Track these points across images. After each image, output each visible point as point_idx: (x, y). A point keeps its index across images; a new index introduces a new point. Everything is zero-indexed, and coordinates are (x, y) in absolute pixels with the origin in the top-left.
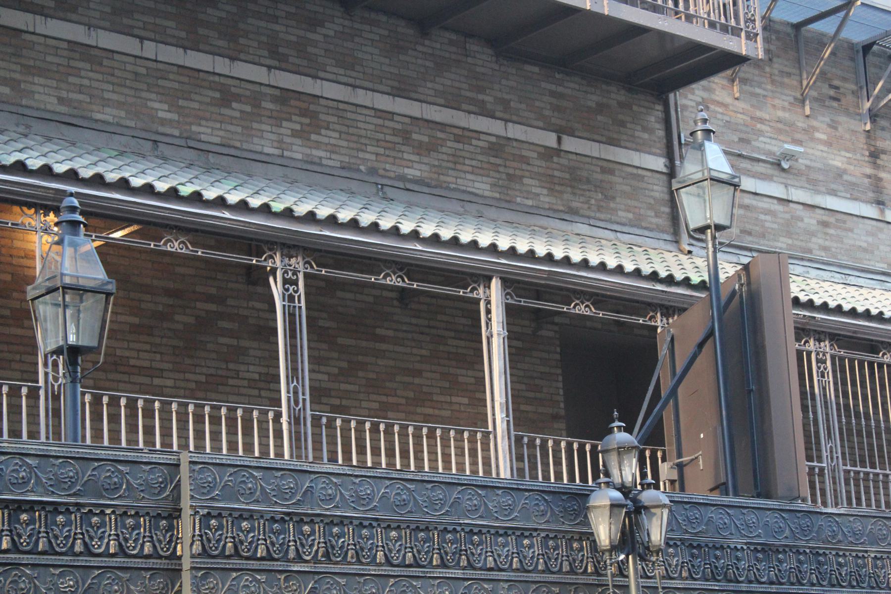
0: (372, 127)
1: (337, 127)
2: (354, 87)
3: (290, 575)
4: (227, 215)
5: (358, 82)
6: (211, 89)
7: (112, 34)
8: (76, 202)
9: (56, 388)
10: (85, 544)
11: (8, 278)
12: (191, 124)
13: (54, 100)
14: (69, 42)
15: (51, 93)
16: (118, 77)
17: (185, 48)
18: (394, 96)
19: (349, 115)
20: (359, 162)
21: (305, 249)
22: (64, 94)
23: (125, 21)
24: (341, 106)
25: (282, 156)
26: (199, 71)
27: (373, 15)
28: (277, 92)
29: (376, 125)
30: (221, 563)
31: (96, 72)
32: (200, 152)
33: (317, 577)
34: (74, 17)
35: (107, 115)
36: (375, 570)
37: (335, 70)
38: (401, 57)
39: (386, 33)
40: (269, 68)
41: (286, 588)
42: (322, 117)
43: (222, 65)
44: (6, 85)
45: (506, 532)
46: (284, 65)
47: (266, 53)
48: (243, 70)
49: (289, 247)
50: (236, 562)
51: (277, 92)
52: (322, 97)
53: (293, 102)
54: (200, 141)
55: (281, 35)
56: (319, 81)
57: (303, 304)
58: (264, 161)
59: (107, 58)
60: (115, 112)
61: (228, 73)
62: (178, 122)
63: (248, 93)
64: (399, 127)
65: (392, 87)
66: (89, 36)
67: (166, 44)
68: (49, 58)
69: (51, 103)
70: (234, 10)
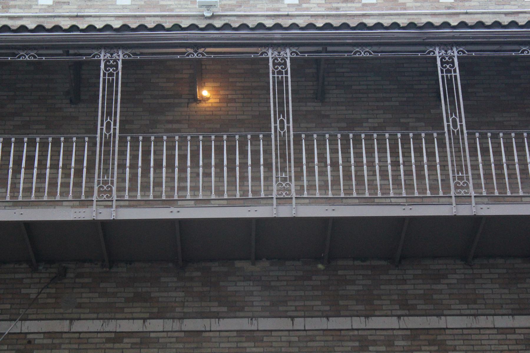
0: (496, 342)
1: (464, 348)
2: (475, 315)
5: (480, 312)
6: (351, 340)
7: (269, 319)
14: (237, 331)
16: (275, 347)
17: (328, 317)
18: (513, 315)
19: (473, 337)
23: (281, 308)
24: (465, 332)
26: (340, 330)
27: (491, 261)
28: (408, 332)
29: (499, 340)
31: (258, 347)
34: (242, 314)
37: (458, 307)
38: (519, 286)
39: (505, 271)
40: (399, 317)
42: (449, 343)
43: (358, 323)
46: (412, 312)
47: (397, 307)
48: (376, 322)
51: (408, 332)
52: (447, 328)
53: (422, 337)
55: (410, 292)
56: (442, 317)
59: (267, 336)
61: (364, 327)
63: (382, 338)
64: (522, 337)
65: (513, 309)
66: (252, 324)
67: (312, 317)
68: (222, 345)
70: (369, 282)
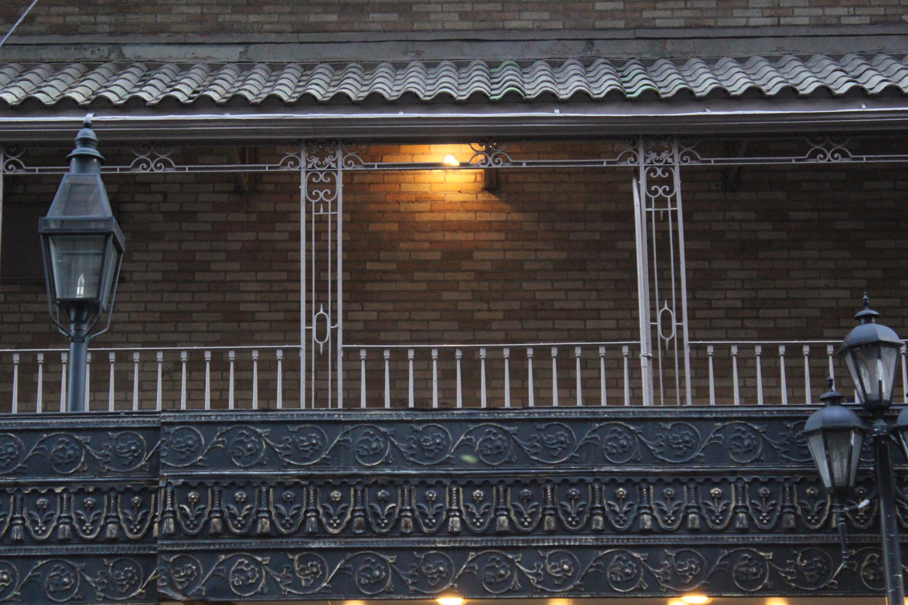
3: (308, 555)
4: (557, 113)
8: (90, 133)
9: (321, 346)
10: (26, 530)
11: (395, 227)
12: (641, 10)
13: (456, 17)
15: (451, 9)
20: (900, 11)
21: (681, 137)
22: (468, 7)
25: (779, 25)
30: (206, 544)
32: (654, 42)
33: (349, 555)
35: (527, 19)
36: (444, 542)
41: (302, 570)
44: (394, 12)
45: (677, 480)
49: (659, 138)
50: (228, 542)
54: (655, 28)
57: (679, 208)
58: (751, 35)
60: (536, 15)
62: (624, 11)
69: (453, 21)
